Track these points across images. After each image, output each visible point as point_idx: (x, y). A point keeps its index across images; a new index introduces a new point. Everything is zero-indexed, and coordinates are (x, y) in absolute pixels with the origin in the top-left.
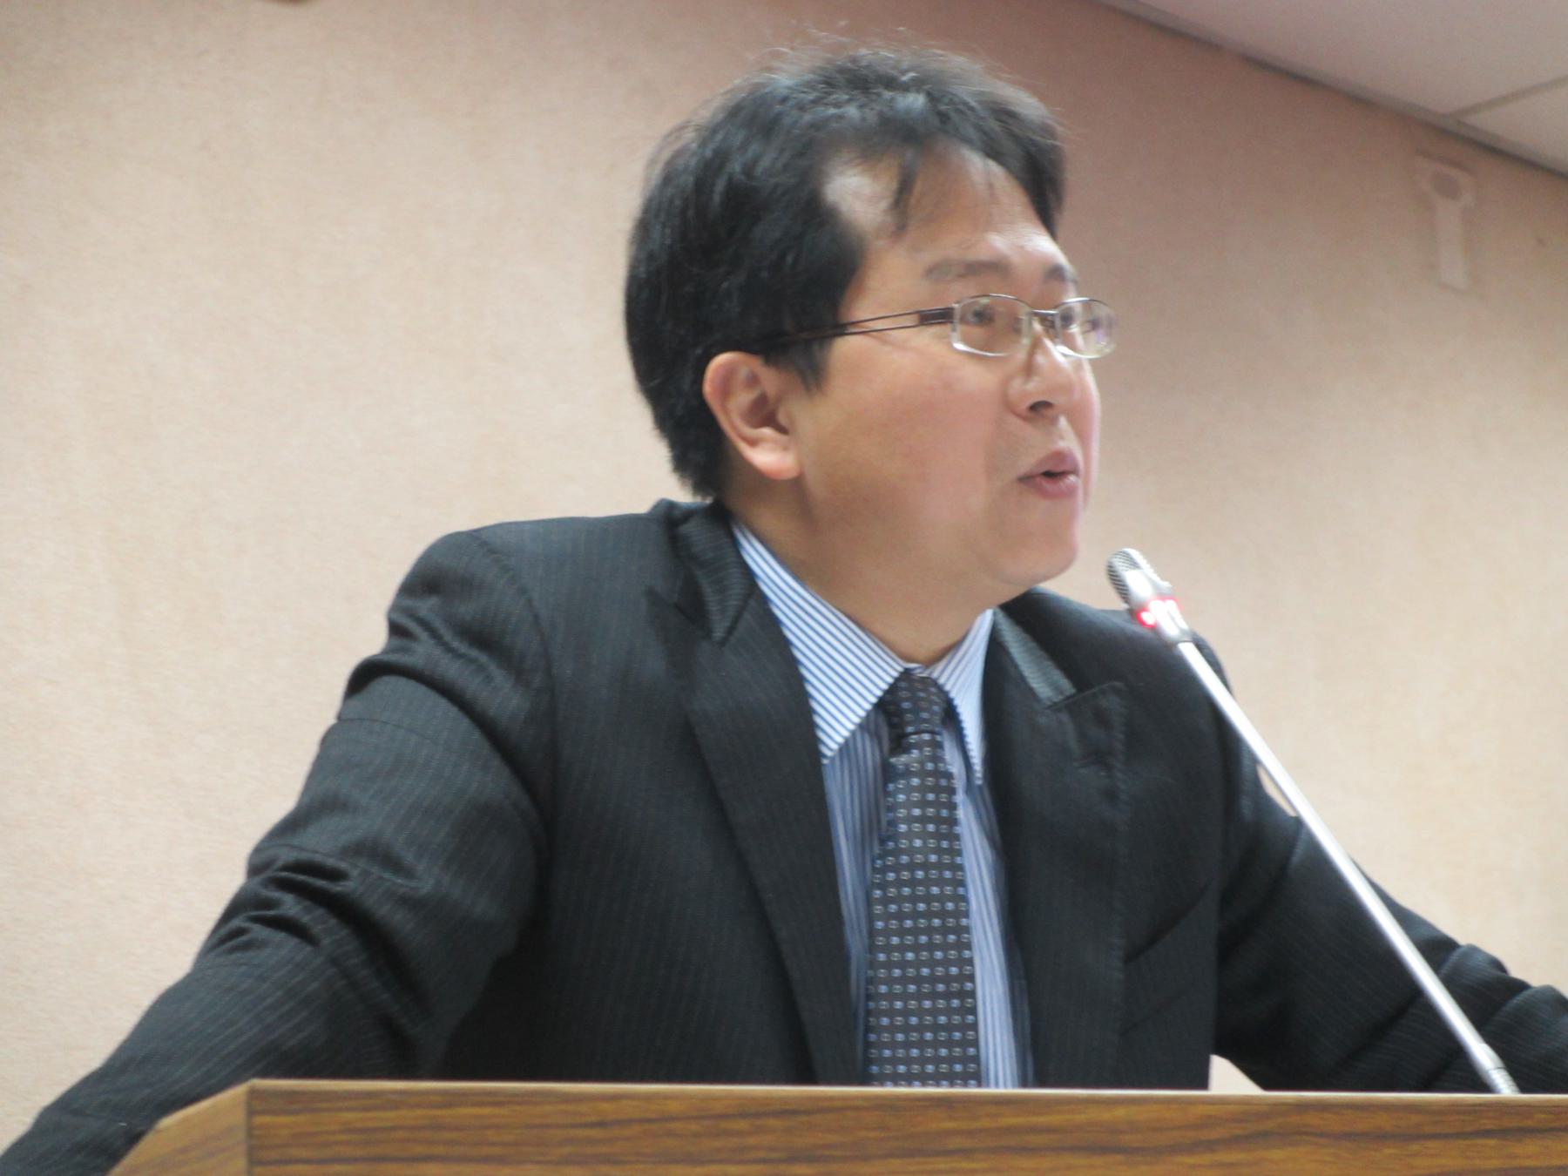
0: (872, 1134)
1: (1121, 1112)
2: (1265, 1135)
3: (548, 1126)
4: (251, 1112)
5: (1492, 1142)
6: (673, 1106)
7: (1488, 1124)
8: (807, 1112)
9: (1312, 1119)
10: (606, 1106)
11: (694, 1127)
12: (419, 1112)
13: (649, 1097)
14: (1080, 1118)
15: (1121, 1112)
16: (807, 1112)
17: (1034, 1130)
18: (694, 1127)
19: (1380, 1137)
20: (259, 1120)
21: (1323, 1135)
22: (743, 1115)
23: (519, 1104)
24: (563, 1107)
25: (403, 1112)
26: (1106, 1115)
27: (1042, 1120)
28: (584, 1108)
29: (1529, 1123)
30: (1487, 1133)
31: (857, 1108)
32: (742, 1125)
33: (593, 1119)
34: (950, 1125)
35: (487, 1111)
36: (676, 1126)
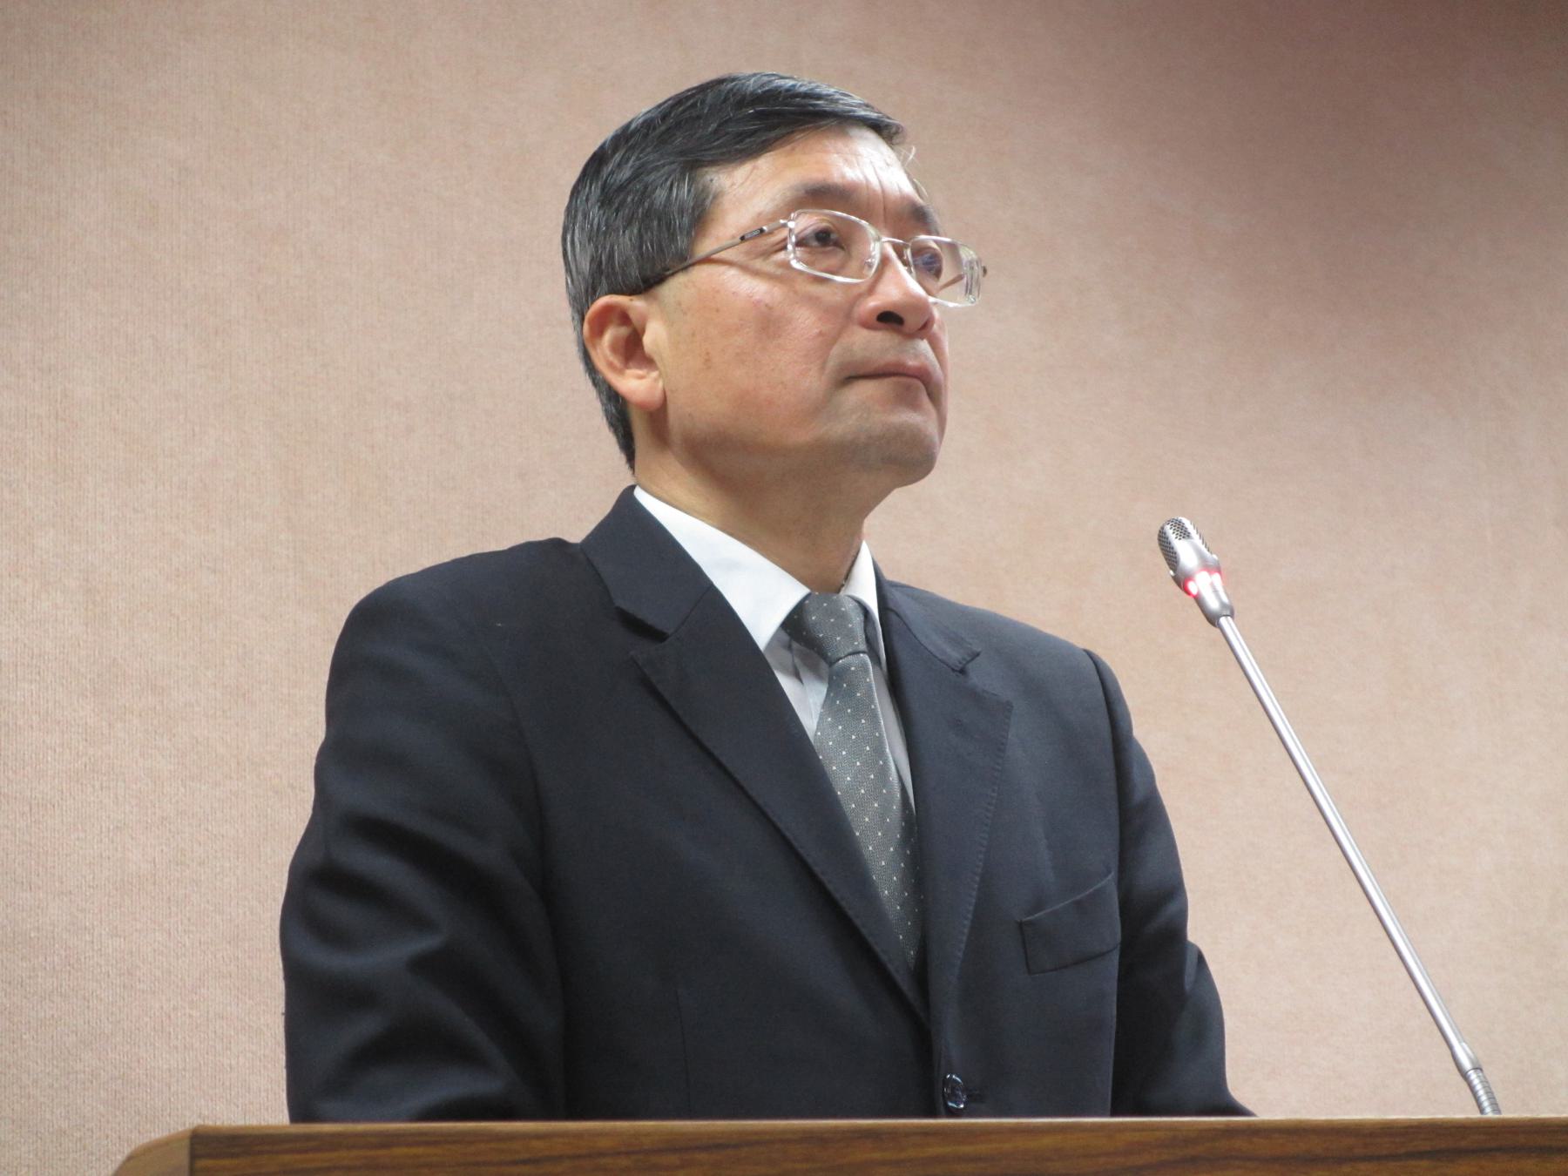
0: (798, 1166)
2: (1194, 1160)
3: (477, 1164)
4: (194, 1156)
5: (1425, 1163)
6: (604, 1144)
8: (736, 1146)
9: (1240, 1144)
12: (354, 1153)
13: (579, 1135)
14: (1007, 1146)
15: (1047, 1141)
16: (736, 1146)
18: (624, 1162)
20: (201, 1163)
21: (1249, 1159)
22: (675, 1150)
24: (493, 1145)
25: (343, 1153)
27: (967, 1149)
29: (1463, 1144)
30: (1421, 1155)
31: (782, 1141)
32: (673, 1159)
33: (527, 1156)
34: (877, 1155)
35: (420, 1150)
36: (602, 1161)
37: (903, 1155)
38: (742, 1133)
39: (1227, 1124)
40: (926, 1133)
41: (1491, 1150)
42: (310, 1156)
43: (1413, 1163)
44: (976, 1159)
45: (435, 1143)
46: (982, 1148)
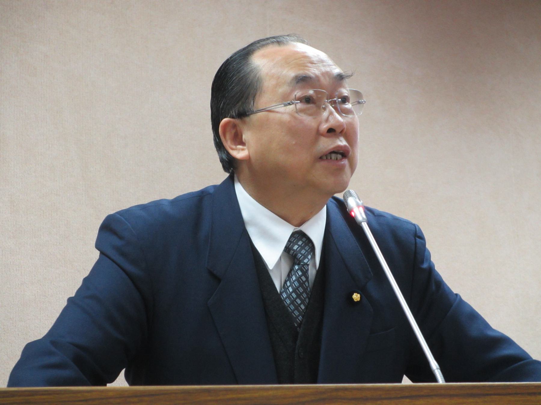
1: (271, 393)
2: (324, 400)
5: (408, 400)
7: (407, 394)
10: (86, 394)
11: (118, 401)
14: (257, 395)
15: (271, 393)
17: (238, 399)
18: (118, 401)
19: (367, 399)
22: (136, 396)
23: (58, 394)
26: (265, 394)
28: (79, 395)
29: (422, 393)
32: (135, 400)
34: (209, 398)
36: (111, 400)
37: (219, 398)
38: (160, 390)
39: (336, 386)
40: (226, 390)
41: (432, 395)
42: (4, 399)
43: (403, 400)
44: (245, 399)
45: (49, 394)
46: (247, 395)
